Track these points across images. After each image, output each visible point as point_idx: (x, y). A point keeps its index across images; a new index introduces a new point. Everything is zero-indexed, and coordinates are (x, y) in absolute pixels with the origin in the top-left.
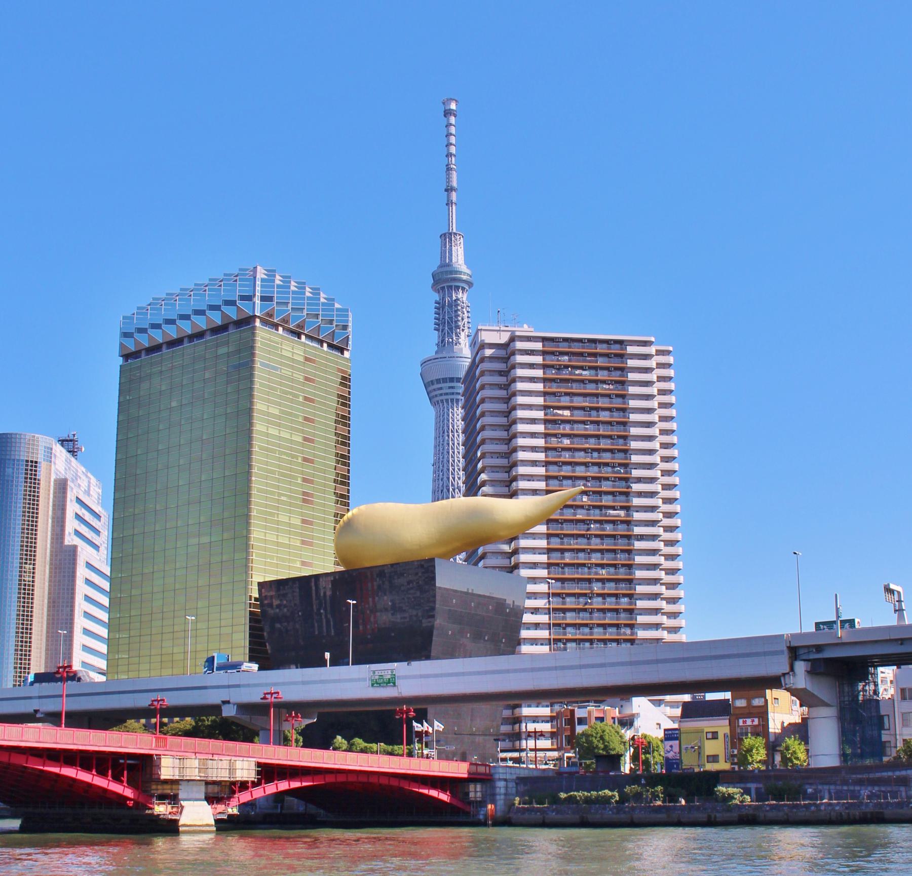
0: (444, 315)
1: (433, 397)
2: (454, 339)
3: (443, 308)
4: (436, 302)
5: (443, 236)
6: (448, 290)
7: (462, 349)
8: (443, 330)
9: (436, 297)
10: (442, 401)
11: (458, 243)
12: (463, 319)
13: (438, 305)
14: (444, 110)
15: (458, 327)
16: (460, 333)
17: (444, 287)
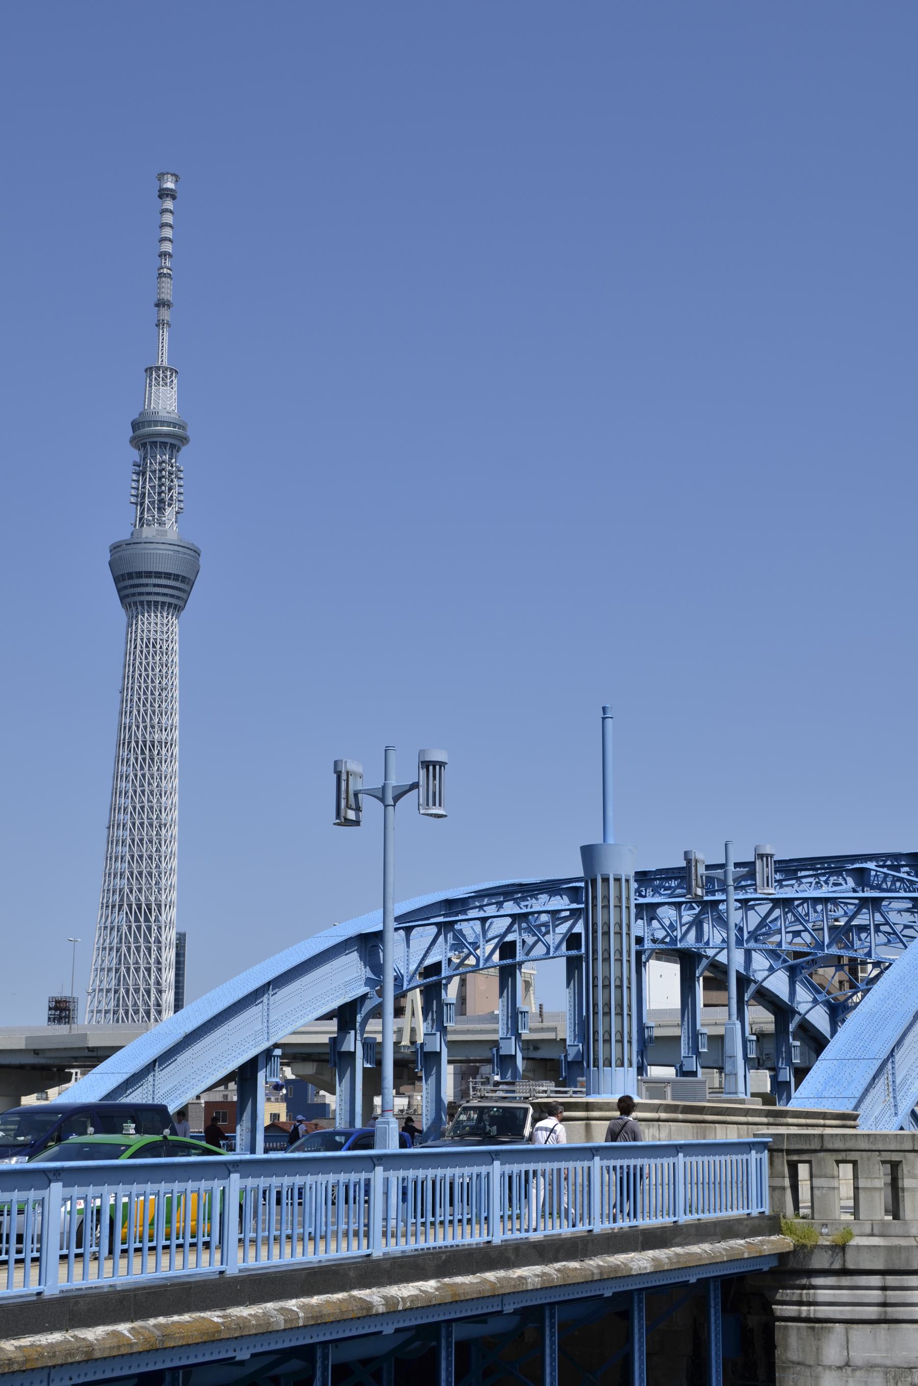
0: (144, 482)
1: (127, 596)
2: (156, 517)
3: (144, 473)
4: (136, 465)
5: (149, 370)
6: (151, 448)
7: (166, 531)
8: (142, 504)
9: (135, 455)
10: (135, 604)
11: (169, 381)
12: (170, 489)
13: (137, 468)
14: (158, 189)
15: (162, 501)
16: (165, 510)
17: (146, 443)
